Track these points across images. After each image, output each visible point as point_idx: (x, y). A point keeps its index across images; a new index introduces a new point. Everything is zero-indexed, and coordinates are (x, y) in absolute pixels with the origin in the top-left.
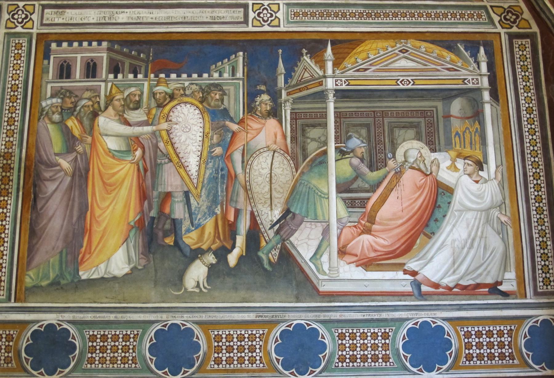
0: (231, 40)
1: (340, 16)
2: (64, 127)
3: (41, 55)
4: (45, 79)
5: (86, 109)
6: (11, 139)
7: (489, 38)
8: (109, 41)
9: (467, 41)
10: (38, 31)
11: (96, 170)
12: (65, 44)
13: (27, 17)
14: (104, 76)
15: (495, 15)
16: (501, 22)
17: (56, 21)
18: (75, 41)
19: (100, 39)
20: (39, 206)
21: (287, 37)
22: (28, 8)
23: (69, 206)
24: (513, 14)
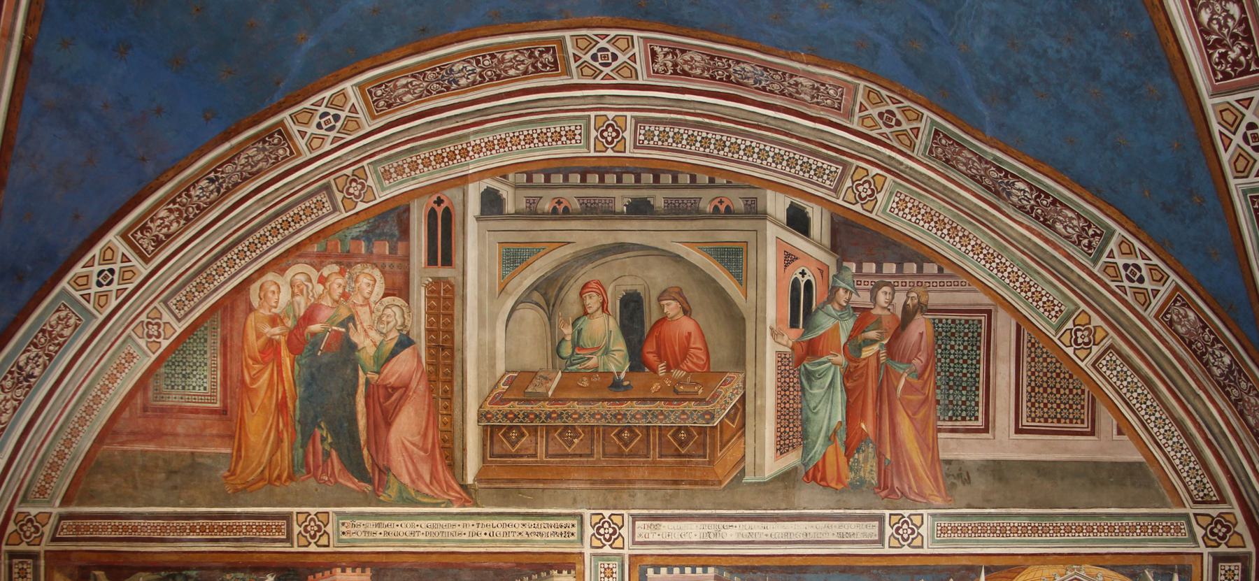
0: (863, 567)
1: (998, 532)
7: (1187, 561)
8: (717, 567)
9: (1157, 565)
12: (664, 570)
13: (614, 533)
15: (1199, 527)
16: (1205, 538)
17: (651, 539)
18: (676, 566)
19: (705, 564)
21: (931, 562)
24: (1223, 526)
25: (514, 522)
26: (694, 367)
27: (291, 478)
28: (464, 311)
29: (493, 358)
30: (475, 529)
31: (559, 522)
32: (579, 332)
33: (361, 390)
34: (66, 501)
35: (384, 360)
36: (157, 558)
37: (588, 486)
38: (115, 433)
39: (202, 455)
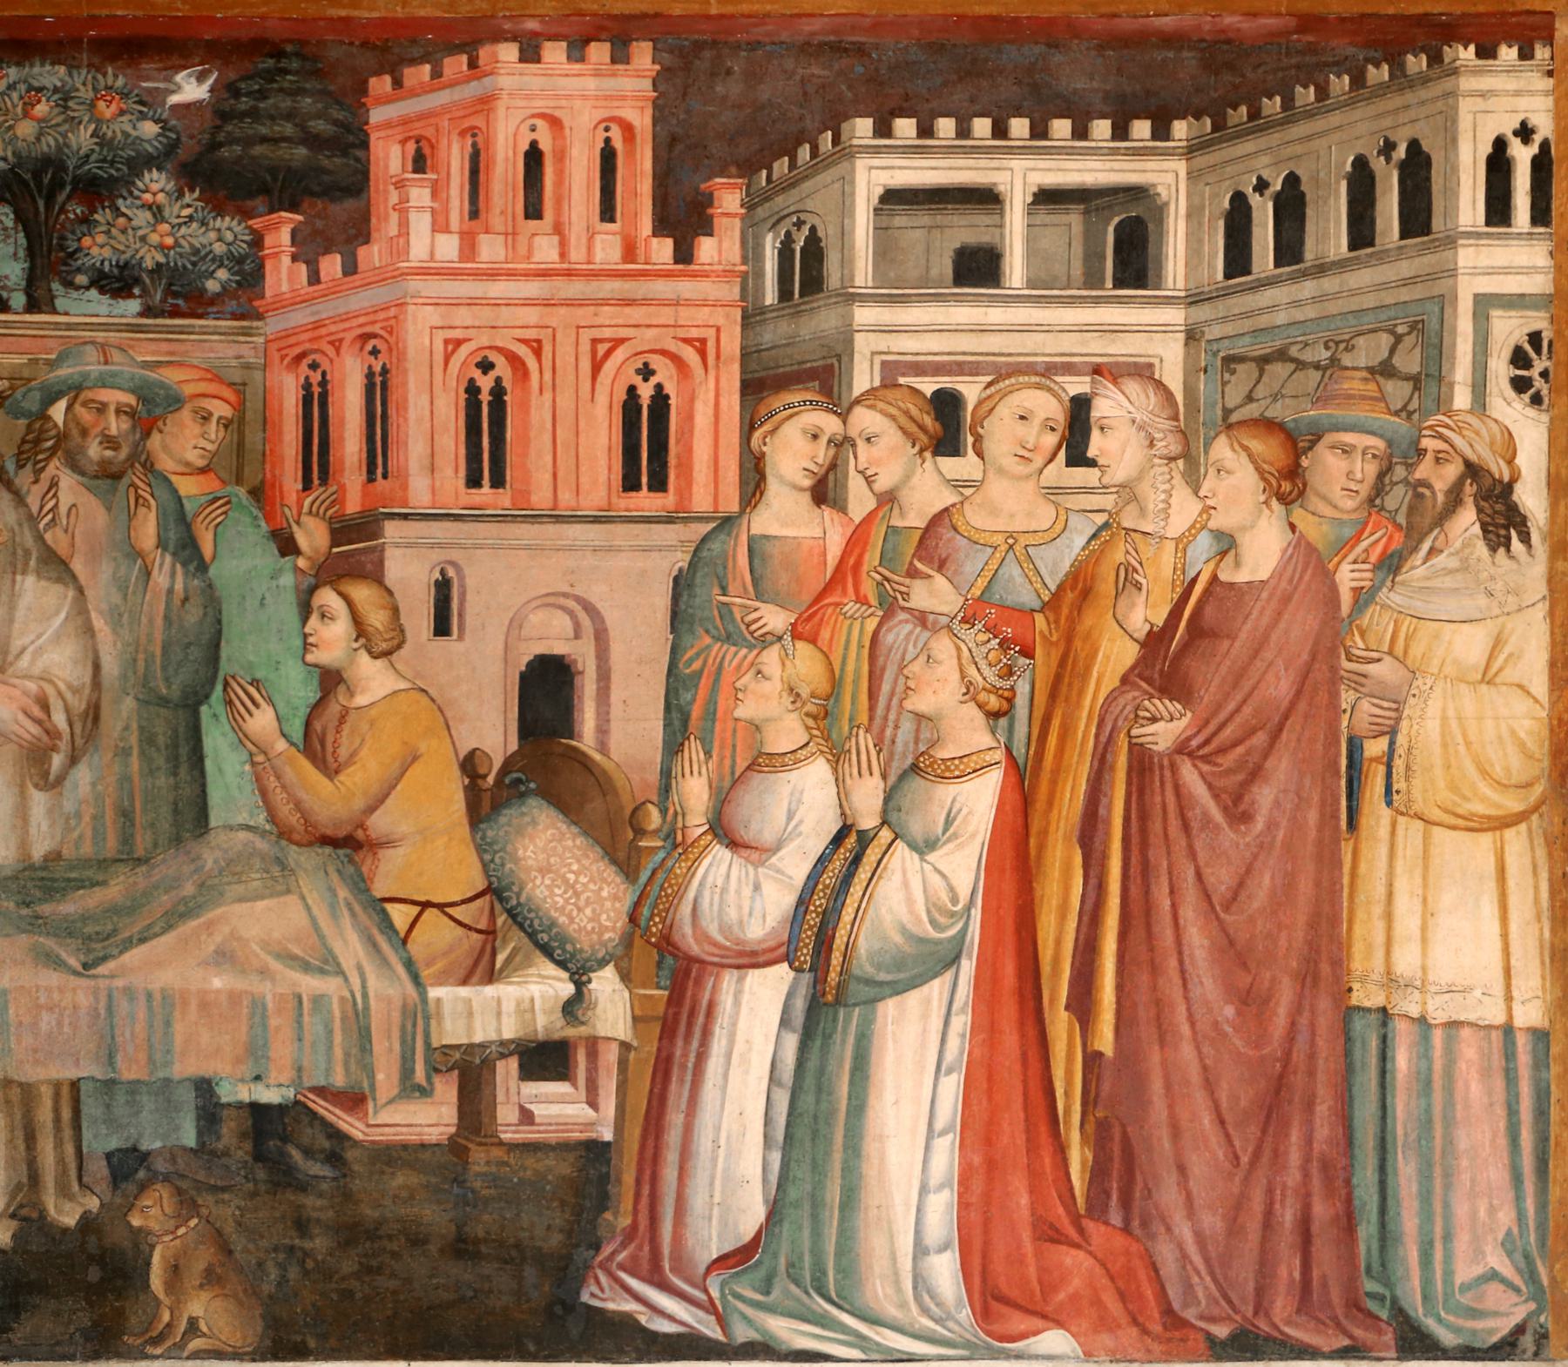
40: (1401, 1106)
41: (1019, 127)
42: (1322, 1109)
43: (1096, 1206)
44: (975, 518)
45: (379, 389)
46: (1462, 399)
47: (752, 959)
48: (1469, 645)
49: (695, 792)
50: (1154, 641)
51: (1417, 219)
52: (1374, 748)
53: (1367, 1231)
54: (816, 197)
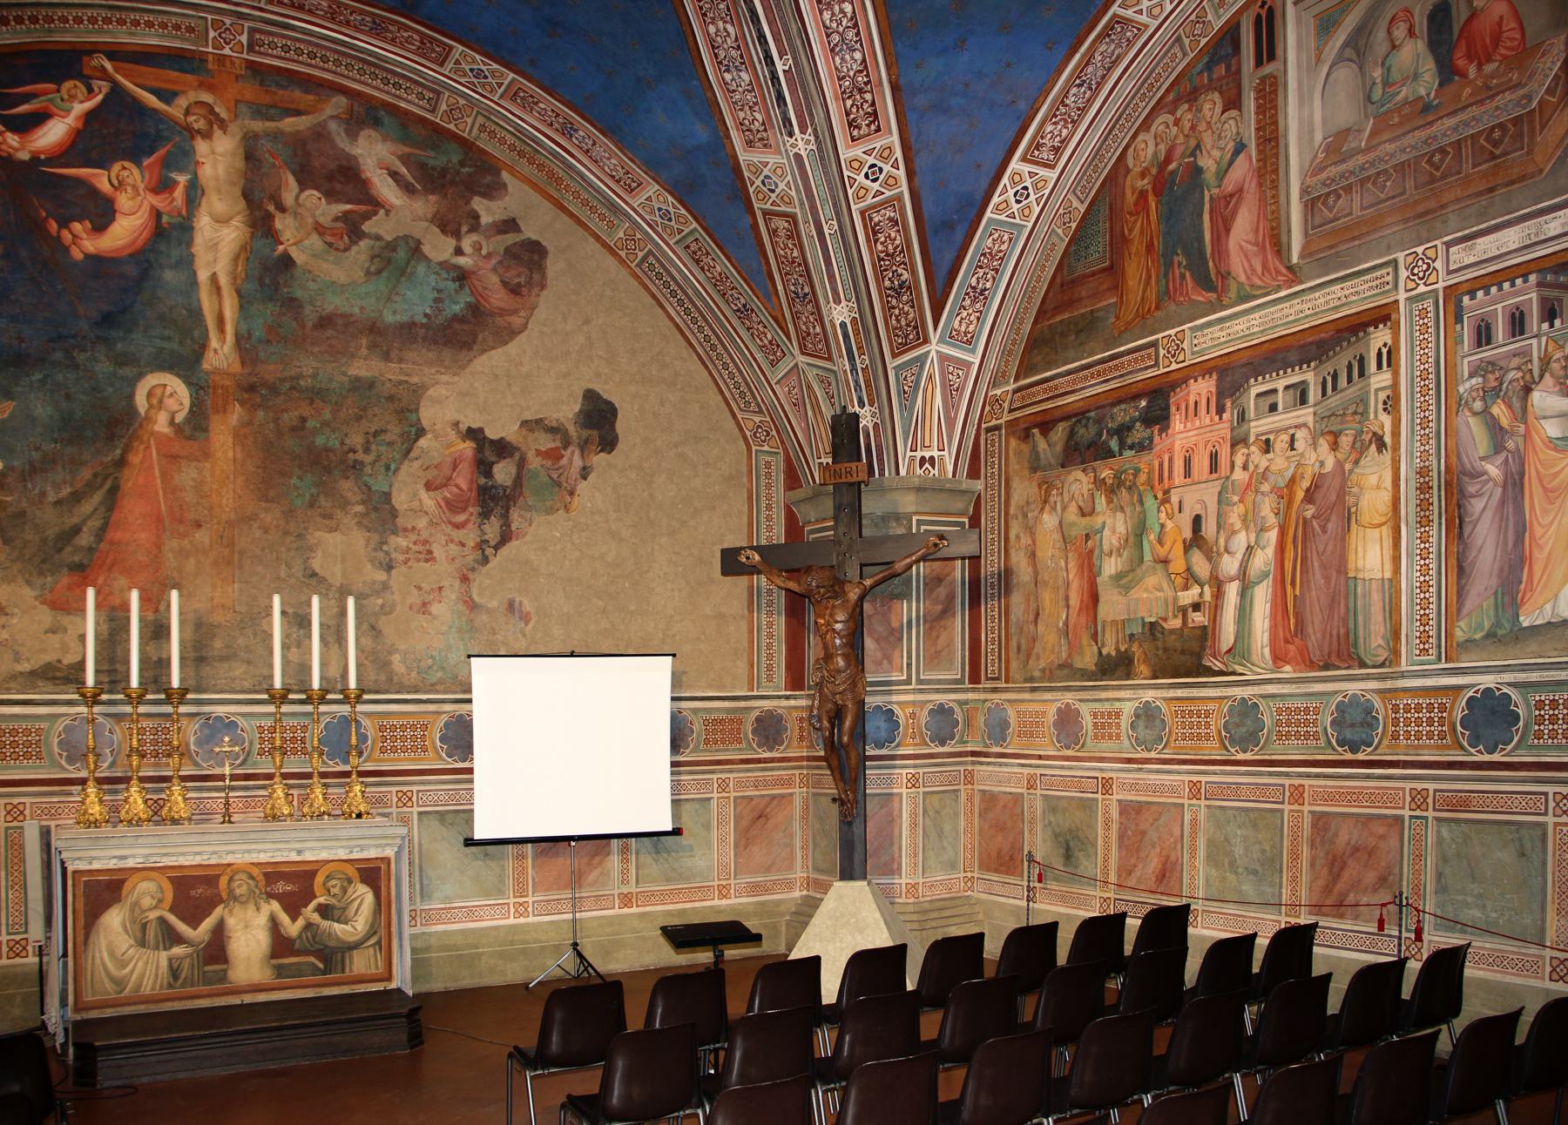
2: (1488, 417)
3: (1451, 319)
4: (1460, 353)
5: (1515, 384)
6: (1427, 448)
8: (1539, 271)
10: (1446, 284)
11: (1534, 474)
12: (1480, 294)
14: (1535, 329)
17: (1467, 261)
20: (1466, 534)
22: (1429, 253)
23: (1502, 529)
25: (1333, 288)
26: (1509, 53)
27: (1157, 308)
28: (1286, 97)
29: (1311, 131)
30: (1299, 307)
31: (1374, 275)
32: (1389, 70)
33: (1207, 207)
34: (1016, 380)
35: (1222, 174)
36: (1070, 408)
37: (1402, 227)
38: (1045, 312)
39: (1098, 310)
40: (1359, 602)
41: (1281, 372)
42: (1342, 605)
43: (1296, 634)
44: (1273, 468)
45: (1171, 460)
46: (1372, 416)
47: (1232, 580)
48: (1373, 480)
49: (1222, 542)
50: (1308, 490)
51: (1362, 374)
52: (1353, 510)
53: (1352, 636)
54: (1243, 399)
